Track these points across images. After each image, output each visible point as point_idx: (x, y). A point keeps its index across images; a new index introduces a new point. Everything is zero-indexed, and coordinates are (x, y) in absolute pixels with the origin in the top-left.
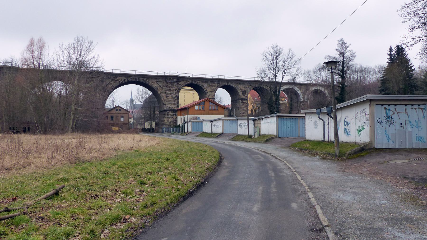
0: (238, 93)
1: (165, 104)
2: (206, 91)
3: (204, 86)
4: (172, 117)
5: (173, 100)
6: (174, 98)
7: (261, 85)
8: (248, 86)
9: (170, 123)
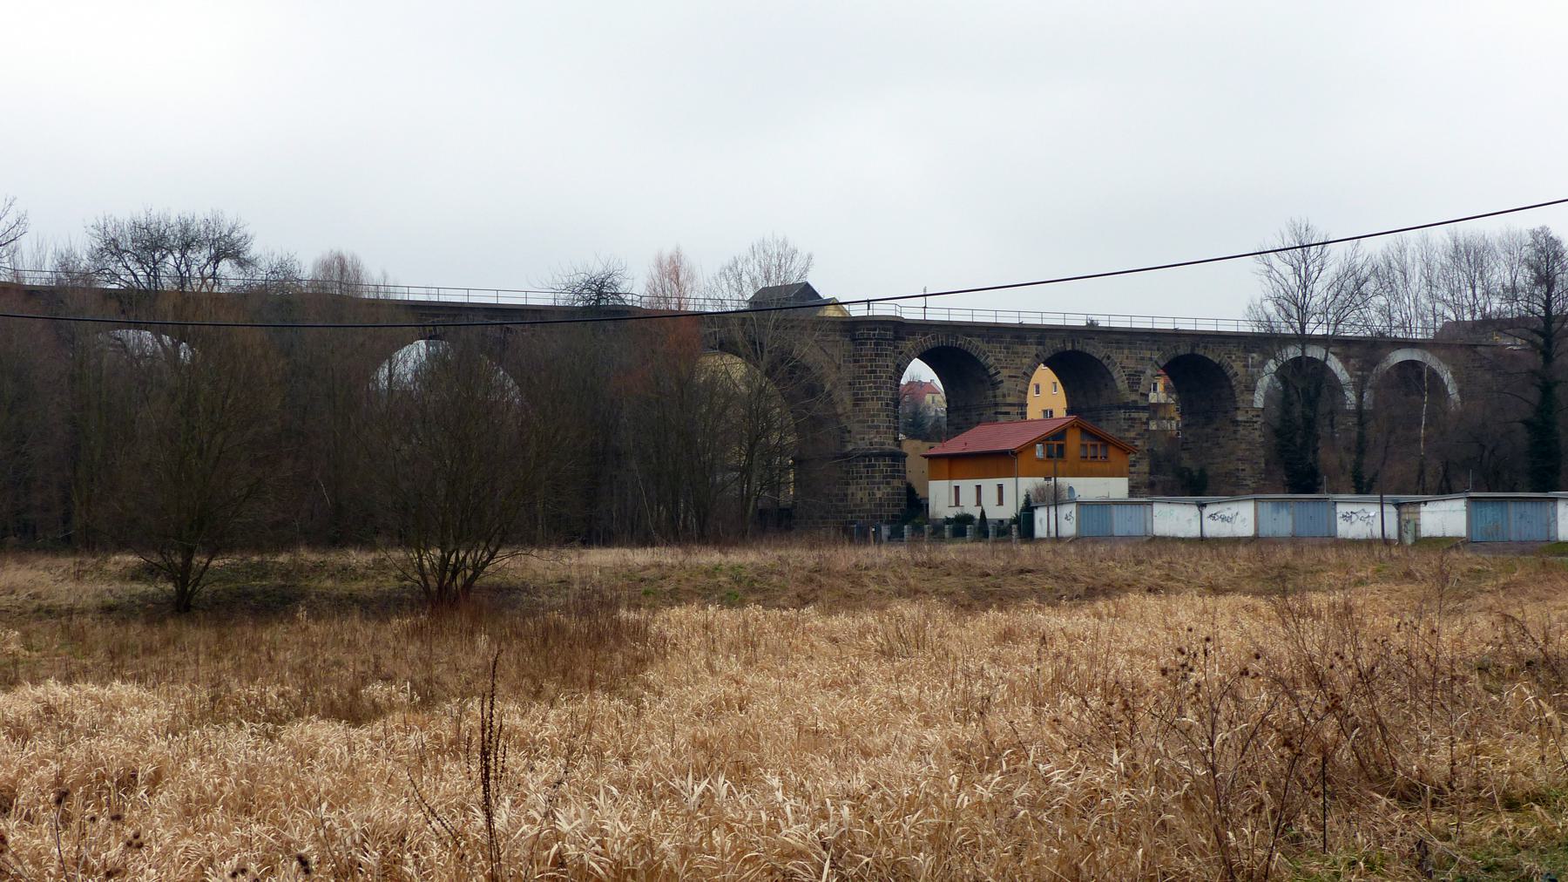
0: (1113, 380)
1: (849, 432)
2: (996, 374)
3: (988, 356)
4: (888, 483)
5: (883, 416)
6: (887, 405)
7: (1198, 345)
8: (1148, 354)
9: (881, 505)
